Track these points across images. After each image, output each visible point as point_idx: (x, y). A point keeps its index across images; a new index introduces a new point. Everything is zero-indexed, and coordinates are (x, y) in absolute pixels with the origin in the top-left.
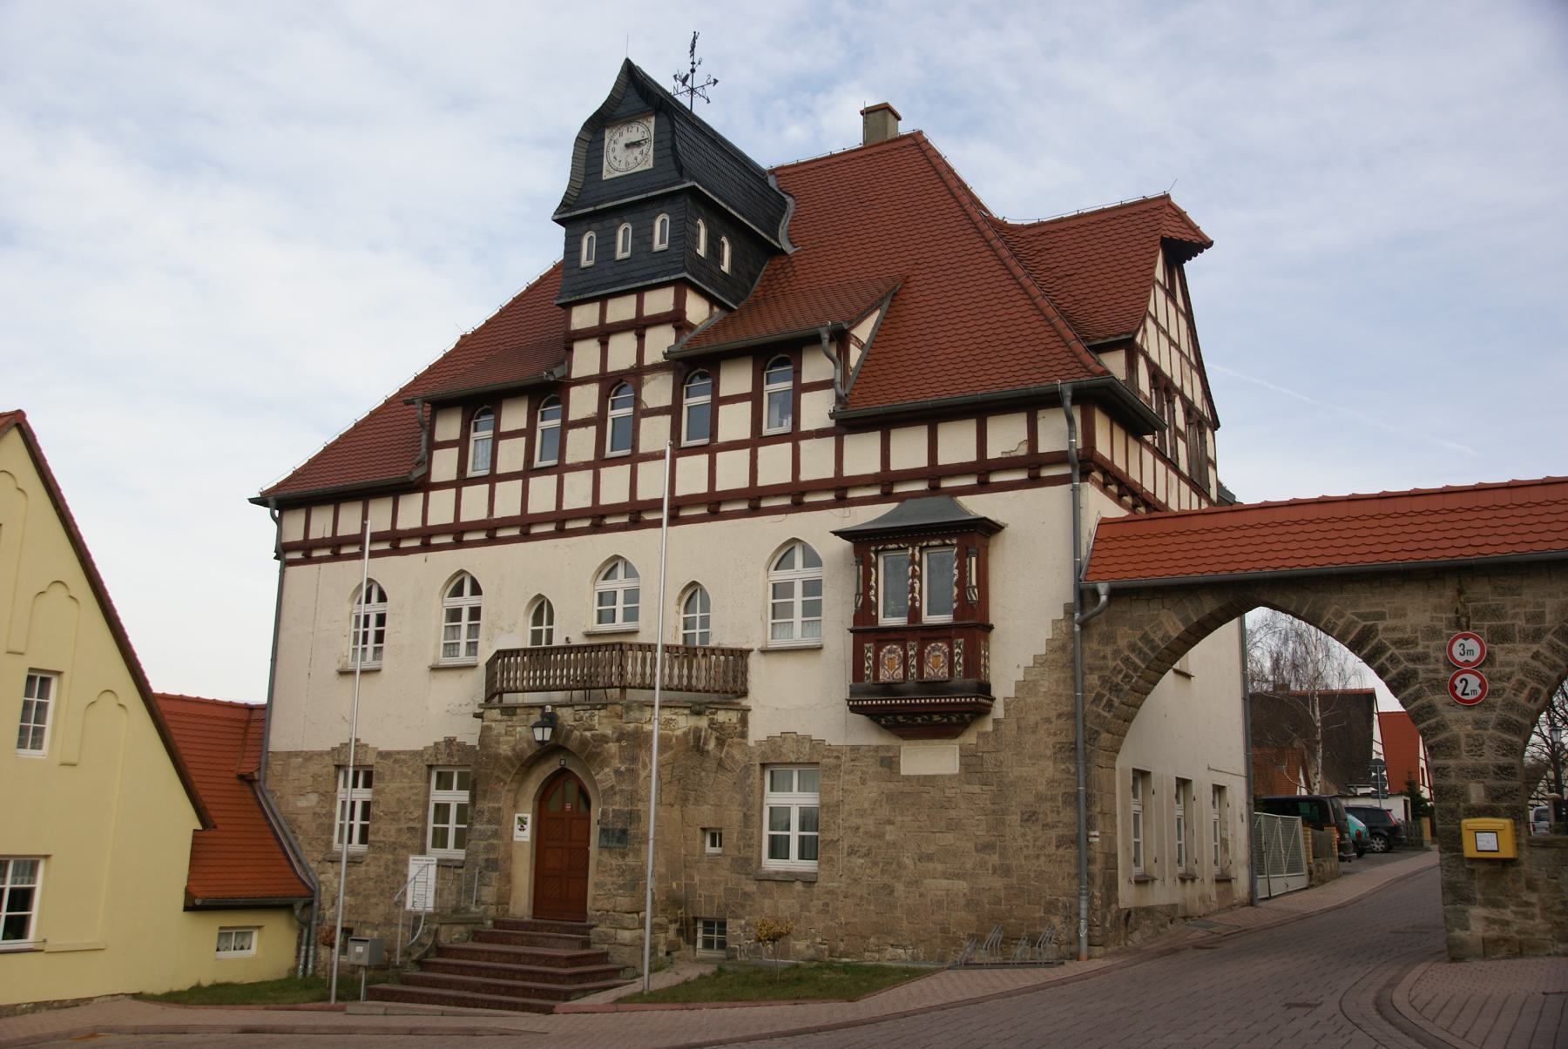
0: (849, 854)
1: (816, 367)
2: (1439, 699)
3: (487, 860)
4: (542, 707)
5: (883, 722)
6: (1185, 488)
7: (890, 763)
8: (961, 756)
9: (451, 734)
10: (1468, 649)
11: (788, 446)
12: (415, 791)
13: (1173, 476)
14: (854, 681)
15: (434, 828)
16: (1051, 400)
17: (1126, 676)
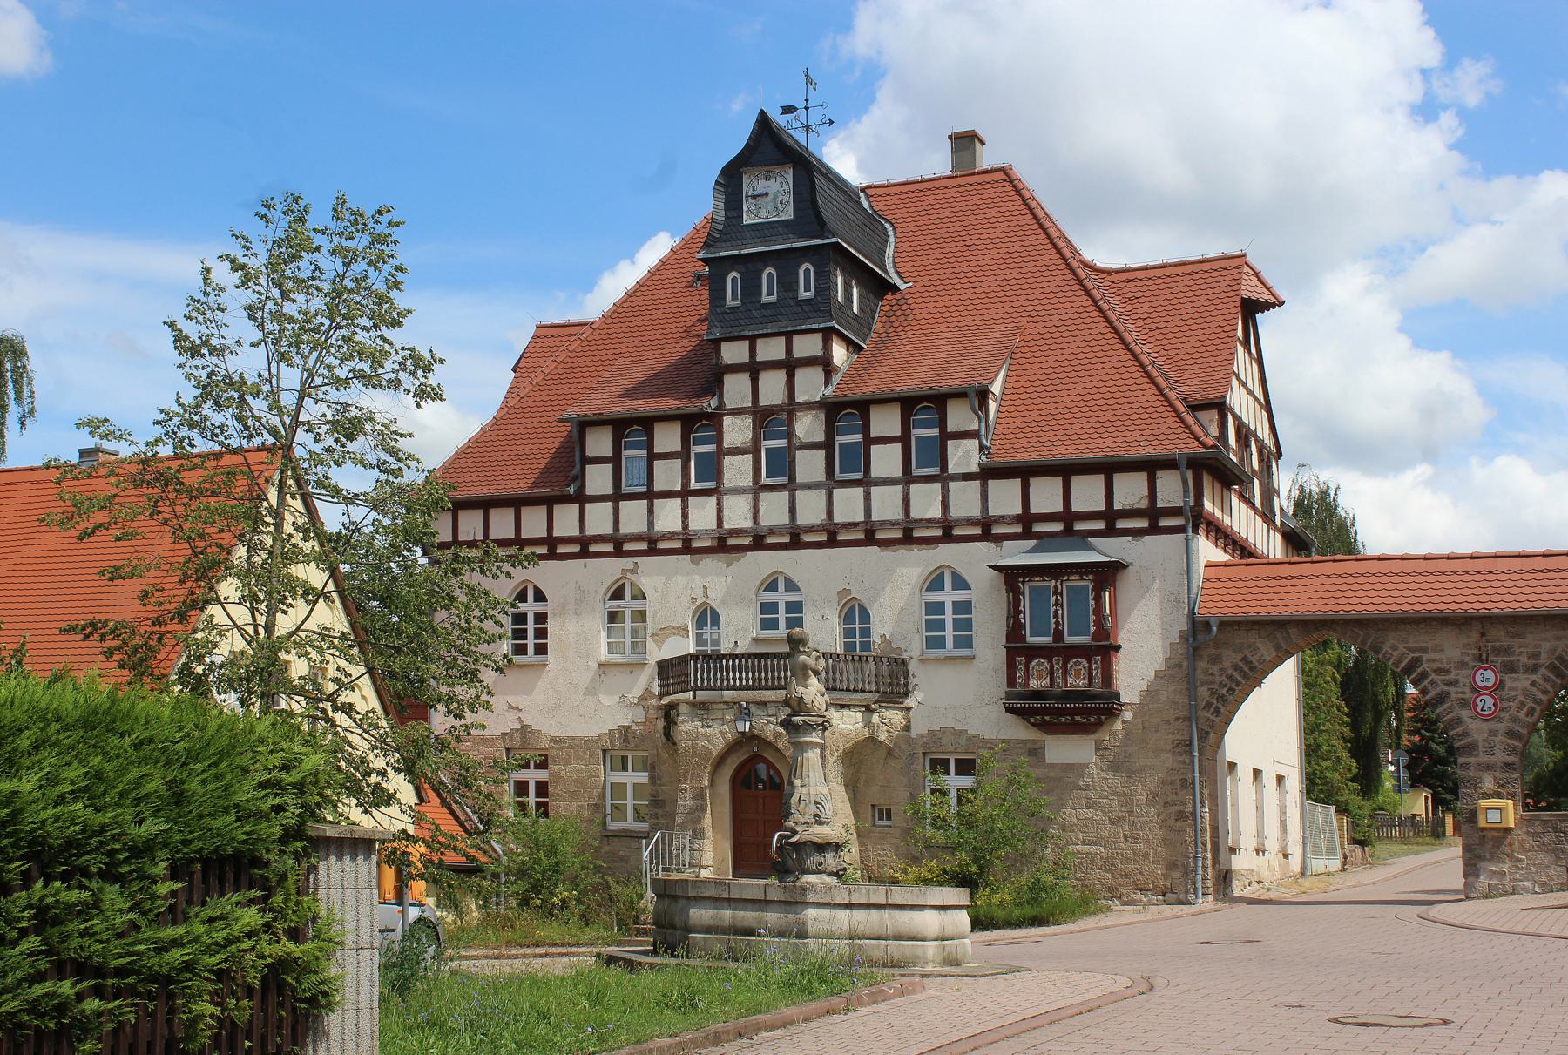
2: (1465, 714)
6: (1259, 520)
7: (1036, 753)
10: (1486, 677)
13: (1251, 513)
16: (1169, 464)
17: (1230, 689)
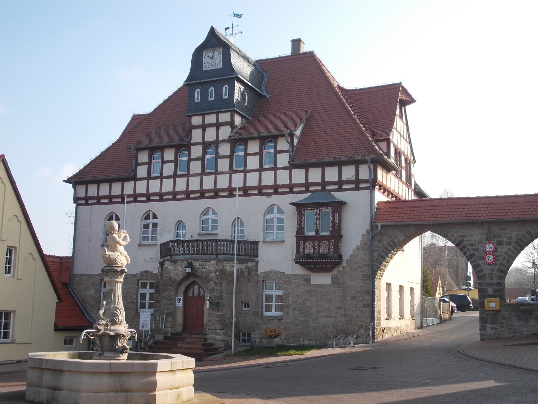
0: (294, 310)
1: (283, 144)
2: (481, 262)
3: (168, 313)
4: (187, 260)
5: (306, 267)
7: (307, 280)
8: (331, 278)
9: (147, 269)
10: (490, 247)
11: (272, 172)
12: (133, 289)
14: (296, 253)
15: (140, 302)
16: (364, 162)
17: (386, 253)
